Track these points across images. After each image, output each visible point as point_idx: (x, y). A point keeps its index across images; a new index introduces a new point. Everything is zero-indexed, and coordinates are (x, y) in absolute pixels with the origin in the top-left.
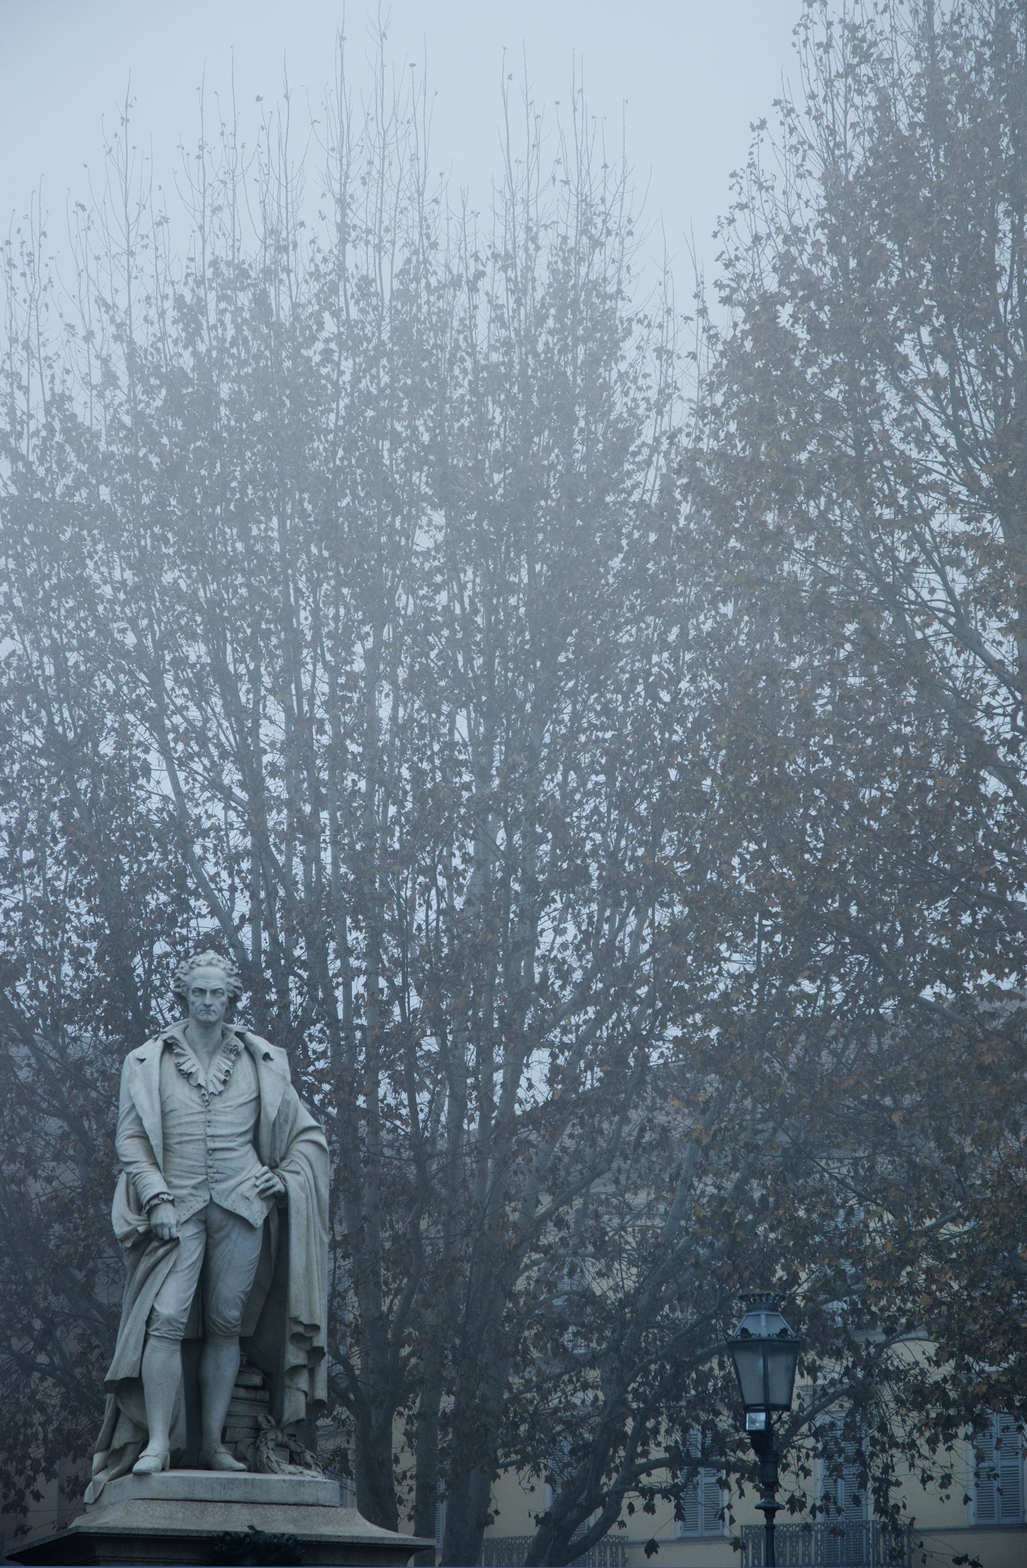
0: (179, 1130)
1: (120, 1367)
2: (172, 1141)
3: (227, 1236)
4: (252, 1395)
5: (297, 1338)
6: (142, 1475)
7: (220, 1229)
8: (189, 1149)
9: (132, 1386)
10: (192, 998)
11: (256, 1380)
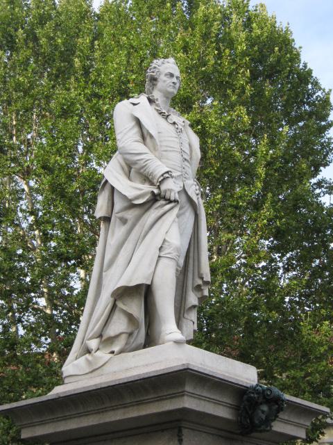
5: (198, 288)
10: (163, 77)
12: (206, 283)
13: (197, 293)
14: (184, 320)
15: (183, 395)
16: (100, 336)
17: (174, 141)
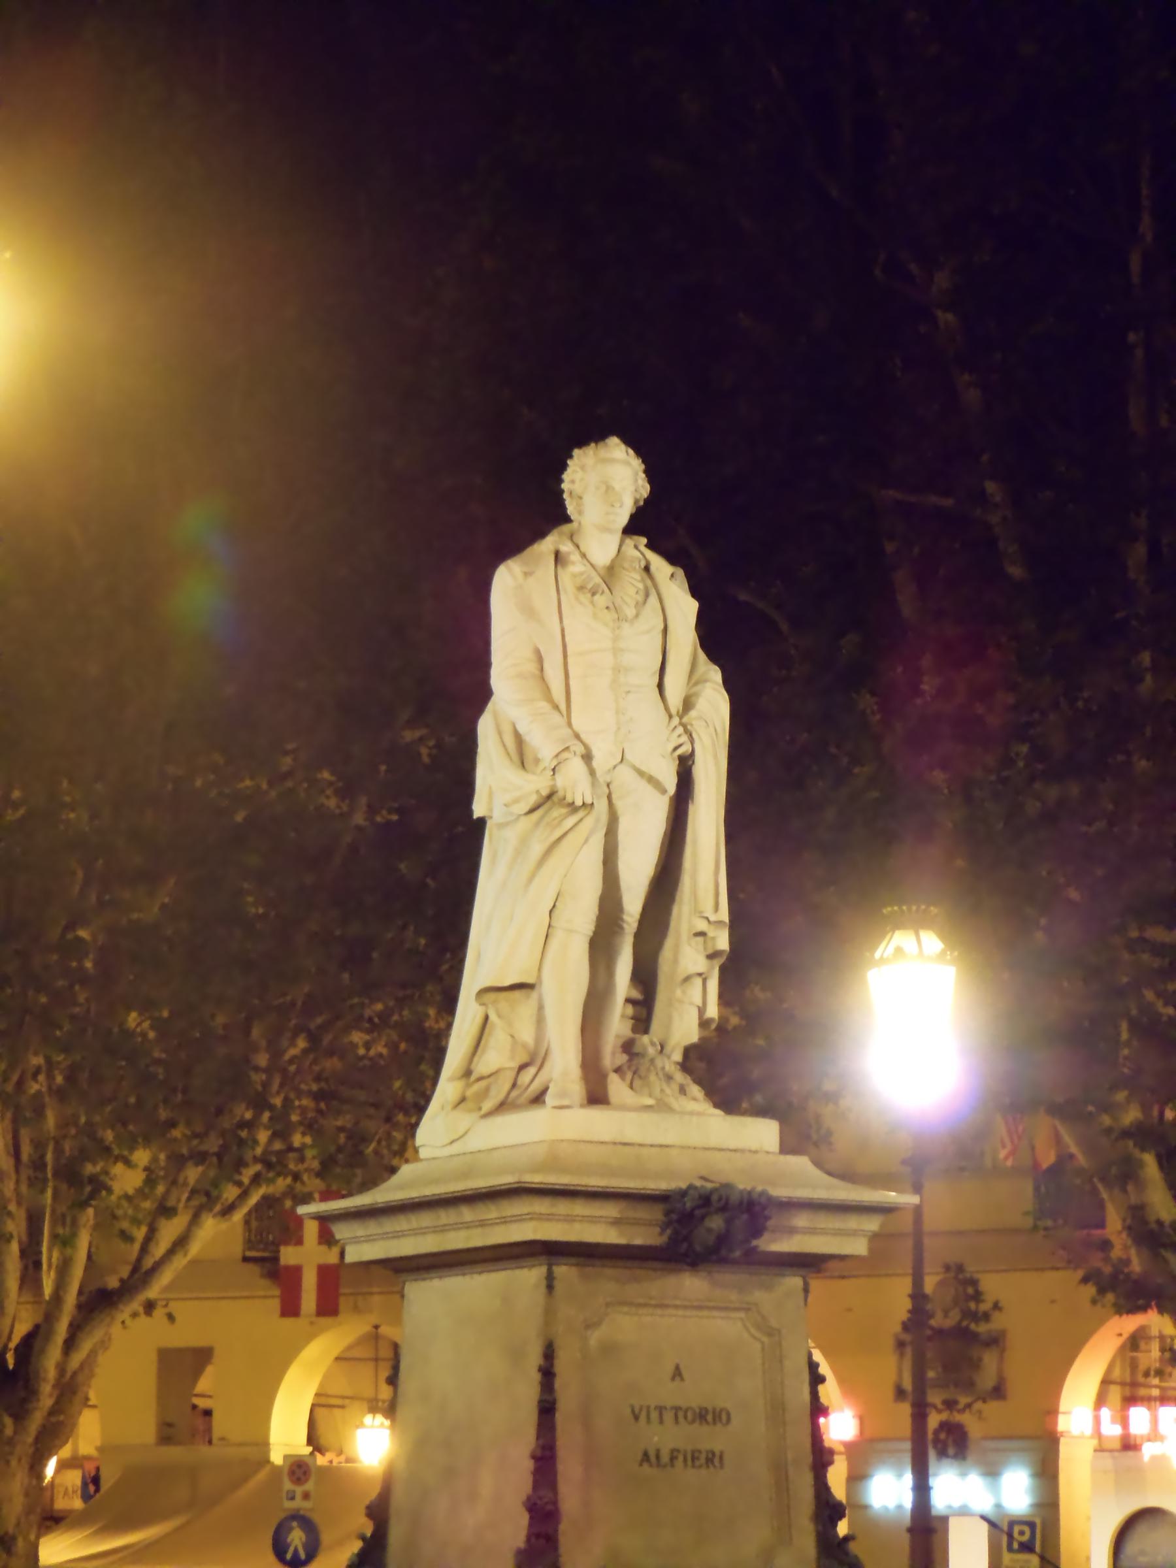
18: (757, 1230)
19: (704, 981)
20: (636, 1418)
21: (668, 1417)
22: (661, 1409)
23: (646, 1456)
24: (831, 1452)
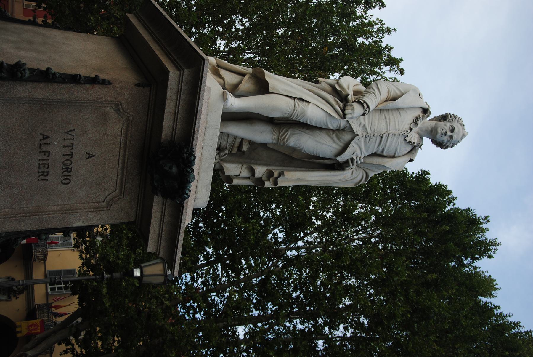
0: (392, 117)
1: (273, 79)
2: (385, 113)
3: (334, 141)
4: (236, 145)
5: (270, 174)
6: (224, 98)
7: (339, 138)
8: (384, 124)
9: (263, 88)
11: (245, 148)
12: (276, 182)
13: (265, 175)
14: (240, 165)
15: (180, 71)
16: (218, 66)
17: (395, 127)
18: (165, 196)
19: (249, 178)
20: (67, 132)
21: (67, 151)
22: (72, 146)
23: (45, 137)
24: (277, 144)
